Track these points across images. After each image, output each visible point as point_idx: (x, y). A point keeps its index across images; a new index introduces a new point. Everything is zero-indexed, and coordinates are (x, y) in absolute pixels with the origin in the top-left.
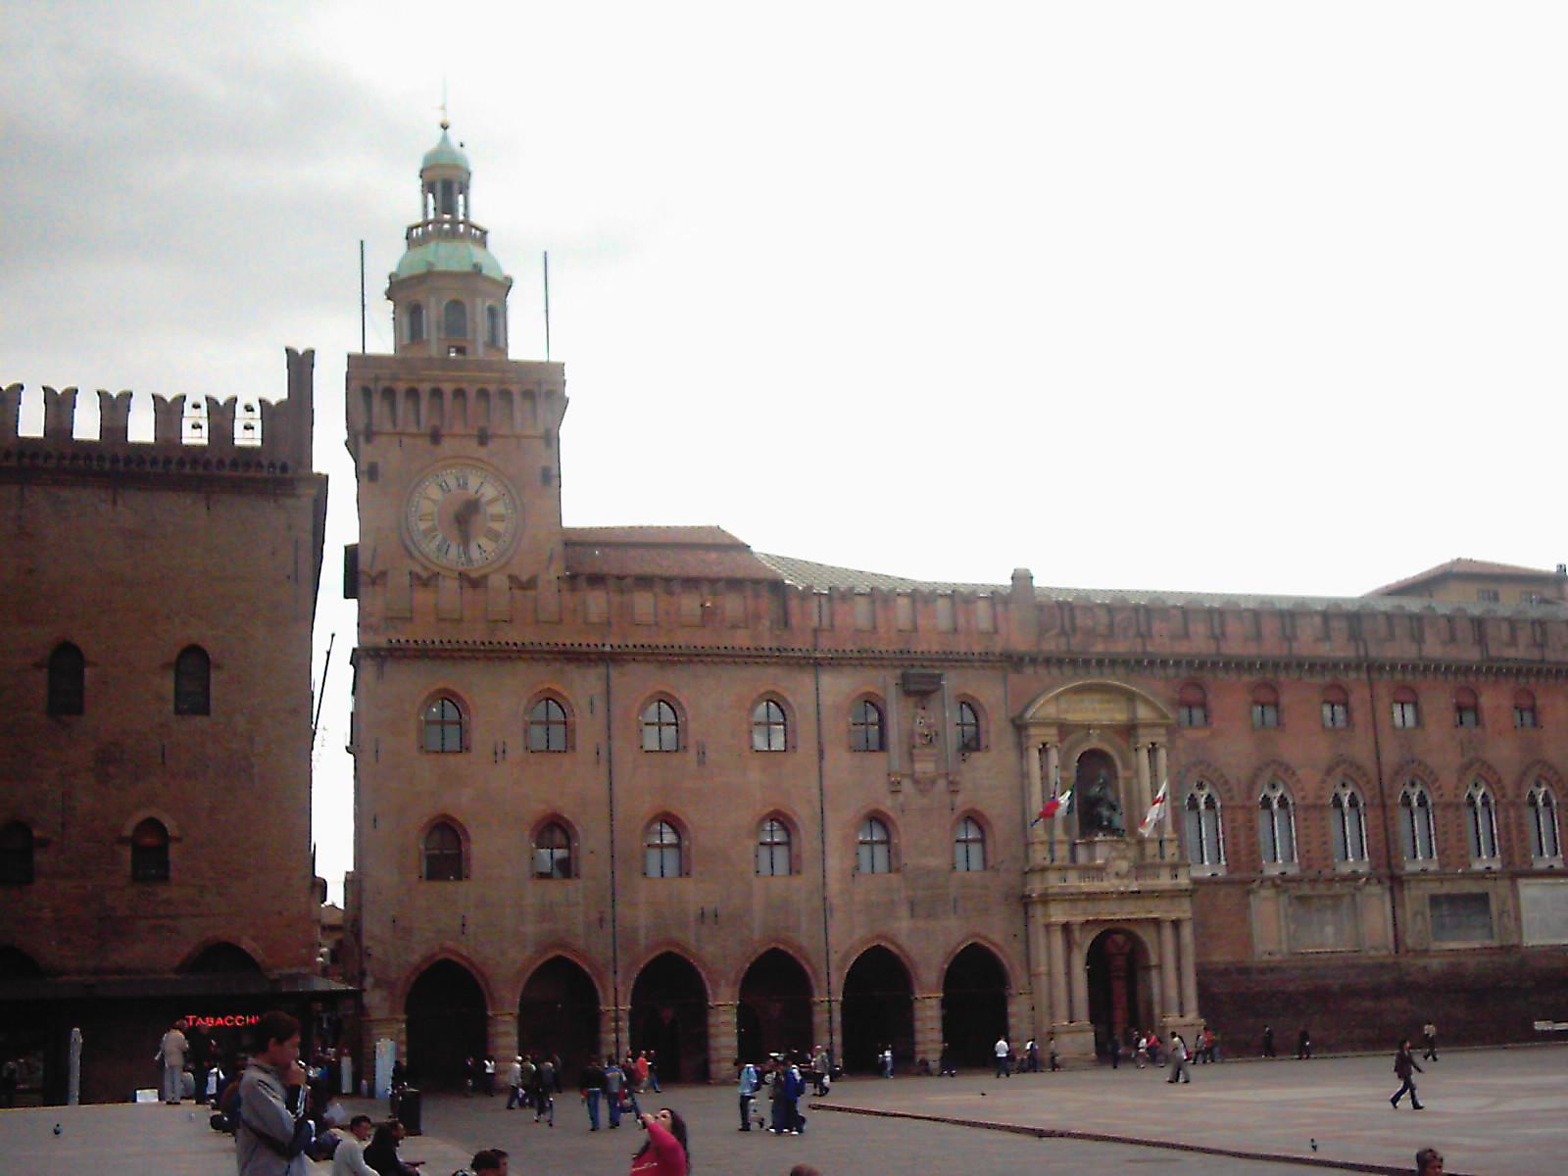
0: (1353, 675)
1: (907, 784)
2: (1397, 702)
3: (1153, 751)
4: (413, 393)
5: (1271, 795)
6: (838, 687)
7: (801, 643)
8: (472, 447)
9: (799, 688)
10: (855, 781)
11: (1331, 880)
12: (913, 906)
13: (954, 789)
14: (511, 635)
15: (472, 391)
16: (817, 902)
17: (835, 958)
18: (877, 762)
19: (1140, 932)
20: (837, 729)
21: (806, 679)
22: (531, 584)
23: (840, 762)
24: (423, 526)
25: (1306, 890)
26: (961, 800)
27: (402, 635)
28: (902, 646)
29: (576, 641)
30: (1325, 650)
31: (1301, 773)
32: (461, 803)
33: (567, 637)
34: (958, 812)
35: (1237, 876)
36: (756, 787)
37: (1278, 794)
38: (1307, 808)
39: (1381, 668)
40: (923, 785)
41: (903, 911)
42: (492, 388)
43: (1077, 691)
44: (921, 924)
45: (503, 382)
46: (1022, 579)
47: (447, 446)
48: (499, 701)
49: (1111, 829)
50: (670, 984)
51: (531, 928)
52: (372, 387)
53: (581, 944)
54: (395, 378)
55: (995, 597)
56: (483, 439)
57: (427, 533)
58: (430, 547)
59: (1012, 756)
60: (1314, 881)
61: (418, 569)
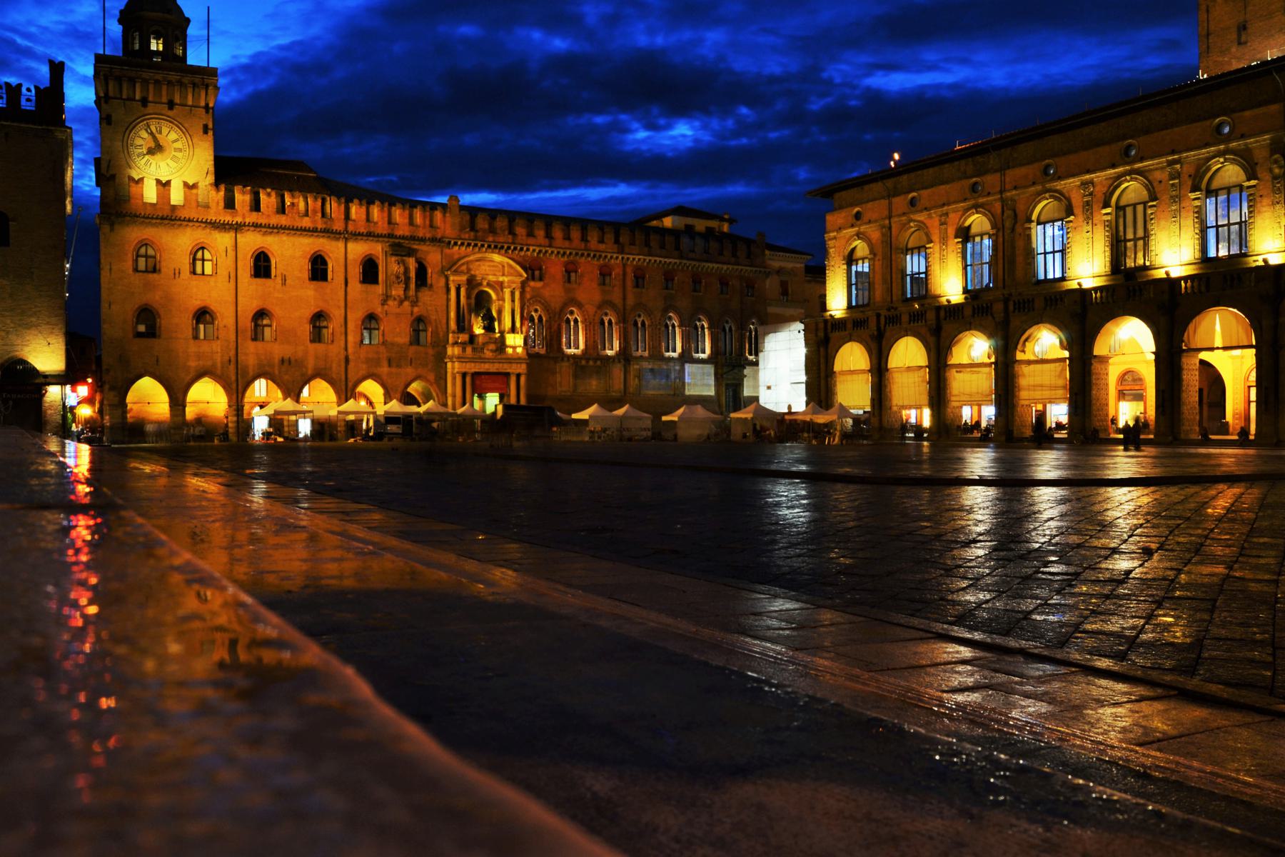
6: (358, 250)
10: (363, 298)
12: (390, 361)
13: (415, 303)
16: (342, 357)
20: (356, 272)
21: (341, 244)
22: (195, 186)
23: (356, 287)
25: (583, 362)
41: (385, 363)
44: (394, 370)
56: (171, 105)
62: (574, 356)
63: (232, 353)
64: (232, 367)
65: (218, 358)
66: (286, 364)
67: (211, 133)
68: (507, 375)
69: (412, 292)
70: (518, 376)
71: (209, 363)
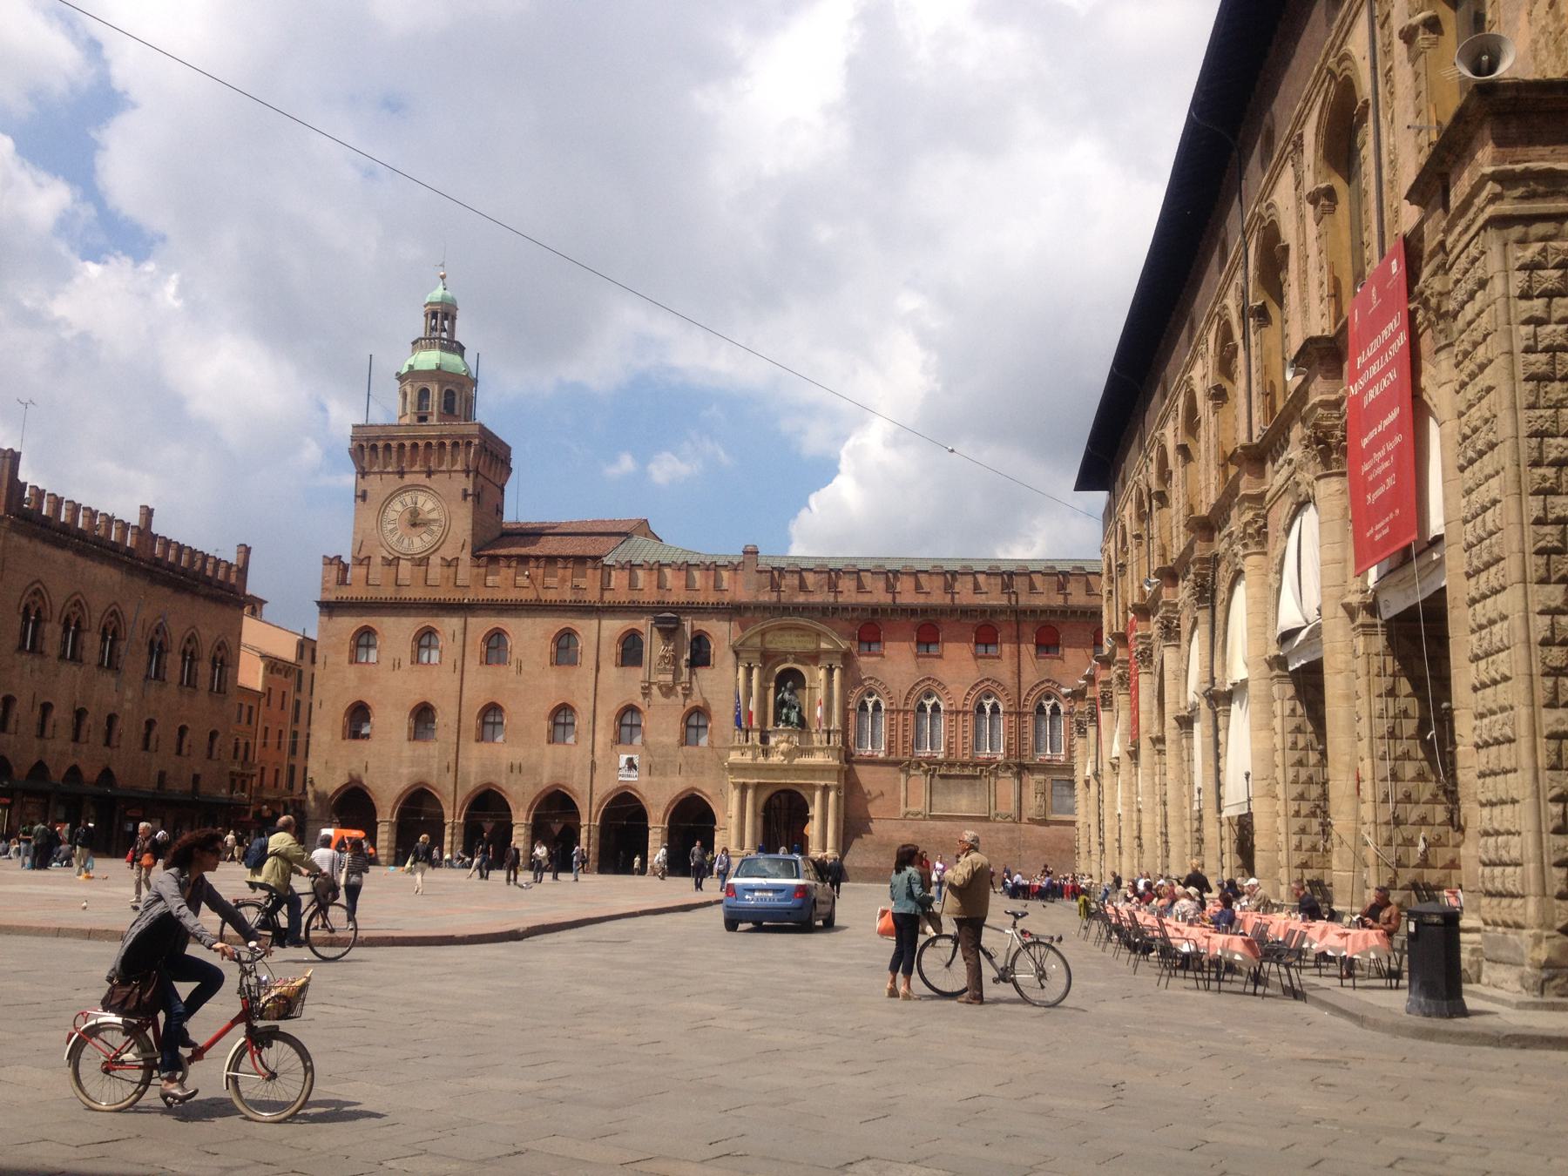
0: (1003, 618)
1: (655, 689)
3: (830, 671)
4: (387, 447)
6: (614, 627)
7: (592, 596)
8: (421, 479)
9: (586, 629)
10: (622, 685)
11: (964, 765)
15: (421, 443)
17: (596, 799)
18: (638, 675)
19: (802, 792)
20: (611, 651)
23: (610, 672)
24: (390, 527)
25: (943, 771)
26: (690, 704)
27: (345, 593)
30: (980, 600)
32: (369, 696)
33: (442, 595)
35: (892, 757)
36: (551, 686)
38: (951, 713)
39: (1024, 612)
40: (668, 691)
42: (434, 442)
43: (782, 628)
44: (655, 779)
45: (440, 437)
46: (751, 553)
47: (408, 479)
48: (397, 632)
49: (787, 722)
50: (488, 807)
51: (405, 771)
53: (433, 781)
54: (378, 438)
56: (429, 474)
59: (731, 671)
60: (951, 765)
61: (385, 554)
62: (932, 761)
64: (452, 774)
66: (516, 771)
67: (470, 499)
70: (826, 789)
71: (424, 770)
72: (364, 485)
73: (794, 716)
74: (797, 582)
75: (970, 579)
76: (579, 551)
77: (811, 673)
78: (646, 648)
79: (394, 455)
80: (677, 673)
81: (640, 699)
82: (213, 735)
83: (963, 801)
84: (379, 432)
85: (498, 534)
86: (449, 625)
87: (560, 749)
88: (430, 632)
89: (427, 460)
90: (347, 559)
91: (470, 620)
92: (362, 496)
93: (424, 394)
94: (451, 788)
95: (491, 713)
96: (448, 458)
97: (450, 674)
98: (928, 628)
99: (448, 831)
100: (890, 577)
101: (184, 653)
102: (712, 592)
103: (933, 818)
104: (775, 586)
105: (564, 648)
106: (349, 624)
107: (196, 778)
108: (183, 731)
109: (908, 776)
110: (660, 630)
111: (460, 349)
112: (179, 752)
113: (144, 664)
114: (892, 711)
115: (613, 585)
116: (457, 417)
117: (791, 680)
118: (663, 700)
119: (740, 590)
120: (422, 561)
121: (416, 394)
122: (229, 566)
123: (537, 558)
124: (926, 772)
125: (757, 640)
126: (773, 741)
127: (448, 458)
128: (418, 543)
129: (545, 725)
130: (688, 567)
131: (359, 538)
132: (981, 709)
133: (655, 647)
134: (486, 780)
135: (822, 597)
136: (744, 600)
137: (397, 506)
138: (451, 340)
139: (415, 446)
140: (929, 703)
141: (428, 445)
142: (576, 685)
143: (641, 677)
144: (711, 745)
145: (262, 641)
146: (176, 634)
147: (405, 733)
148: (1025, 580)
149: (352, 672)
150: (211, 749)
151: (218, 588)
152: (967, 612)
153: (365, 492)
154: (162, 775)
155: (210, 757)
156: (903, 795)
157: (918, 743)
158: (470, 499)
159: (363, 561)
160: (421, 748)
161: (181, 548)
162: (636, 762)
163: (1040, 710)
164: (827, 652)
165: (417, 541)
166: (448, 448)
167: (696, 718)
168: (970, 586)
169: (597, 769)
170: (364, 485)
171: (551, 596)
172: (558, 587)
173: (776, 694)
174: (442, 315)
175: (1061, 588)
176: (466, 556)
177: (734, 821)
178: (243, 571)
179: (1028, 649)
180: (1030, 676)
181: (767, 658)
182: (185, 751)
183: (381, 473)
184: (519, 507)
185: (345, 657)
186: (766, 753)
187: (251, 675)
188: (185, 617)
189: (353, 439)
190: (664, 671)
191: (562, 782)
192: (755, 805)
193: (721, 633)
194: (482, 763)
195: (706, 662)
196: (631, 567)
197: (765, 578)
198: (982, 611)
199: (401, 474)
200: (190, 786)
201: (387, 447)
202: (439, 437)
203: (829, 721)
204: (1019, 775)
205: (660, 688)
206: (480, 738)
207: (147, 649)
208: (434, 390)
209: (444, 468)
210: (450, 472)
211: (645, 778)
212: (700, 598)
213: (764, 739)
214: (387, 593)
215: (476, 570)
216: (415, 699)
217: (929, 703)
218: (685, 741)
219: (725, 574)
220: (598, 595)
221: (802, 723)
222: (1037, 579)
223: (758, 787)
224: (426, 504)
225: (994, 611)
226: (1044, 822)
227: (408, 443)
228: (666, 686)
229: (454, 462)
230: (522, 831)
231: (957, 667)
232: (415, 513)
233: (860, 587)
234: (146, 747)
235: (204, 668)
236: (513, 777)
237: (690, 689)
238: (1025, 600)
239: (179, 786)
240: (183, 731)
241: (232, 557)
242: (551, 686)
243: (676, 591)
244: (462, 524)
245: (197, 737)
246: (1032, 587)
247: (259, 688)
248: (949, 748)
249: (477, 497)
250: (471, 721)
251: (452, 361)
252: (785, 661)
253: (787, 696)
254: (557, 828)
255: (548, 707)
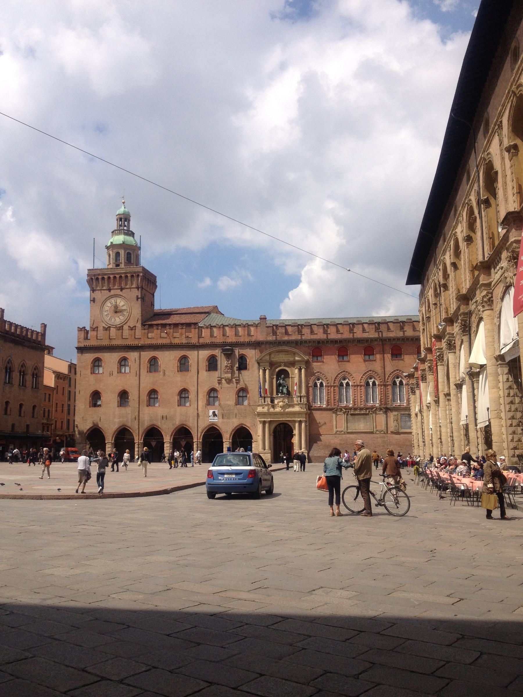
0: (376, 343)
1: (223, 381)
2: (367, 355)
3: (300, 370)
4: (103, 278)
5: (343, 382)
6: (204, 354)
7: (194, 340)
8: (118, 292)
9: (192, 355)
10: (209, 379)
11: (361, 409)
14: (115, 343)
15: (118, 276)
18: (216, 374)
19: (290, 424)
20: (204, 364)
23: (204, 374)
25: (352, 412)
26: (239, 386)
27: (88, 343)
28: (224, 340)
29: (132, 343)
30: (366, 335)
31: (354, 375)
32: (99, 388)
33: (129, 342)
34: (238, 388)
36: (179, 381)
37: (346, 382)
38: (355, 386)
39: (386, 340)
40: (229, 381)
42: (123, 275)
44: (225, 420)
45: (125, 273)
46: (263, 319)
47: (113, 292)
48: (110, 359)
49: (282, 393)
51: (117, 420)
52: (93, 277)
53: (129, 424)
54: (99, 275)
55: (256, 326)
56: (122, 289)
57: (106, 315)
58: (107, 319)
59: (257, 371)
60: (355, 409)
61: (104, 325)
62: (346, 408)
63: (137, 413)
64: (136, 422)
65: (129, 417)
67: (139, 300)
68: (295, 422)
69: (236, 375)
70: (300, 422)
71: (125, 419)
72: (94, 295)
73: (285, 391)
74: (284, 331)
75: (360, 326)
76: (188, 321)
77: (292, 371)
78: (219, 363)
79: (106, 282)
80: (233, 373)
81: (217, 385)
82: (34, 407)
83: (361, 425)
84: (99, 272)
85: (152, 315)
86: (133, 356)
87: (183, 409)
88: (125, 359)
89: (120, 284)
90: (88, 328)
91: (142, 353)
92: (93, 300)
93: (118, 254)
94: (137, 427)
95: (153, 394)
96: (129, 282)
97: (134, 377)
98: (343, 349)
99: (136, 446)
100: (325, 327)
101: (20, 372)
102: (246, 336)
103: (348, 433)
104: (274, 333)
105: (183, 364)
106: (90, 357)
107: (28, 426)
108: (21, 405)
109: (337, 415)
110: (224, 354)
111: (132, 234)
112: (20, 415)
113: (3, 377)
114: (328, 386)
115: (203, 335)
116: (132, 264)
117: (283, 374)
118: (228, 385)
119: (259, 335)
120: (120, 328)
121: (114, 254)
122: (38, 333)
123: (170, 325)
124: (344, 413)
125: (267, 357)
126: (276, 402)
127: (129, 282)
128: (118, 320)
129: (177, 398)
130: (236, 326)
131: (93, 319)
132: (368, 384)
133: (223, 362)
134: (151, 423)
135: (295, 337)
136: (261, 340)
137: (108, 304)
138: (128, 230)
139: (115, 277)
140: (344, 382)
141: (121, 277)
142: (188, 380)
143: (217, 376)
144: (249, 404)
145: (53, 365)
146: (17, 363)
147: (116, 404)
148: (385, 325)
149: (92, 378)
150: (33, 413)
151: (32, 343)
152: (360, 341)
153: (94, 298)
154: (13, 425)
155: (33, 417)
156: (334, 423)
157: (340, 400)
158: (139, 300)
159: (95, 329)
160: (123, 410)
161: (17, 326)
162: (217, 413)
163: (394, 383)
164: (299, 361)
165: (117, 319)
166: (129, 278)
167: (242, 393)
168: (361, 329)
169: (200, 417)
170: (94, 295)
171: (176, 341)
172: (180, 337)
173: (277, 381)
174: (124, 219)
175: (402, 328)
176: (139, 325)
177: (260, 438)
178: (44, 335)
179: (388, 356)
180: (389, 368)
181: (272, 365)
182: (22, 415)
183: (101, 290)
184: (162, 301)
185: (89, 371)
186: (273, 407)
187: (49, 380)
188: (19, 356)
189: (88, 275)
190: (227, 373)
191: (184, 423)
192: (269, 431)
193: (251, 355)
194: (150, 416)
195: (245, 368)
196: (211, 327)
197: (270, 330)
198: (367, 340)
199: (110, 290)
200: (25, 430)
201: (103, 278)
202: (124, 273)
203: (300, 392)
204: (386, 413)
205: (226, 380)
206: (149, 405)
207: (4, 371)
208: (122, 252)
209: (128, 287)
210: (130, 288)
211: (221, 420)
212: (242, 340)
213: (272, 401)
214: (106, 343)
215: (143, 331)
216: (120, 389)
217: (344, 382)
218: (238, 403)
219: (252, 329)
220: (197, 340)
221: (289, 393)
222: (391, 325)
223: (270, 422)
224: (121, 303)
225: (372, 340)
226: (398, 433)
227: (112, 276)
228: (228, 379)
229: (132, 284)
230: (168, 445)
231: (357, 365)
232: (116, 307)
233: (312, 332)
234: (6, 413)
235: (29, 378)
236: (163, 422)
237: (239, 380)
238: (386, 334)
239: (20, 430)
240: (21, 405)
241: (39, 329)
242: (179, 381)
243: (231, 337)
244: (136, 311)
245: (27, 408)
246: (389, 329)
247: (53, 386)
248: (354, 402)
249: (143, 299)
250: (144, 397)
251: (129, 239)
252: (280, 366)
253: (281, 381)
254: (183, 443)
255: (177, 390)
